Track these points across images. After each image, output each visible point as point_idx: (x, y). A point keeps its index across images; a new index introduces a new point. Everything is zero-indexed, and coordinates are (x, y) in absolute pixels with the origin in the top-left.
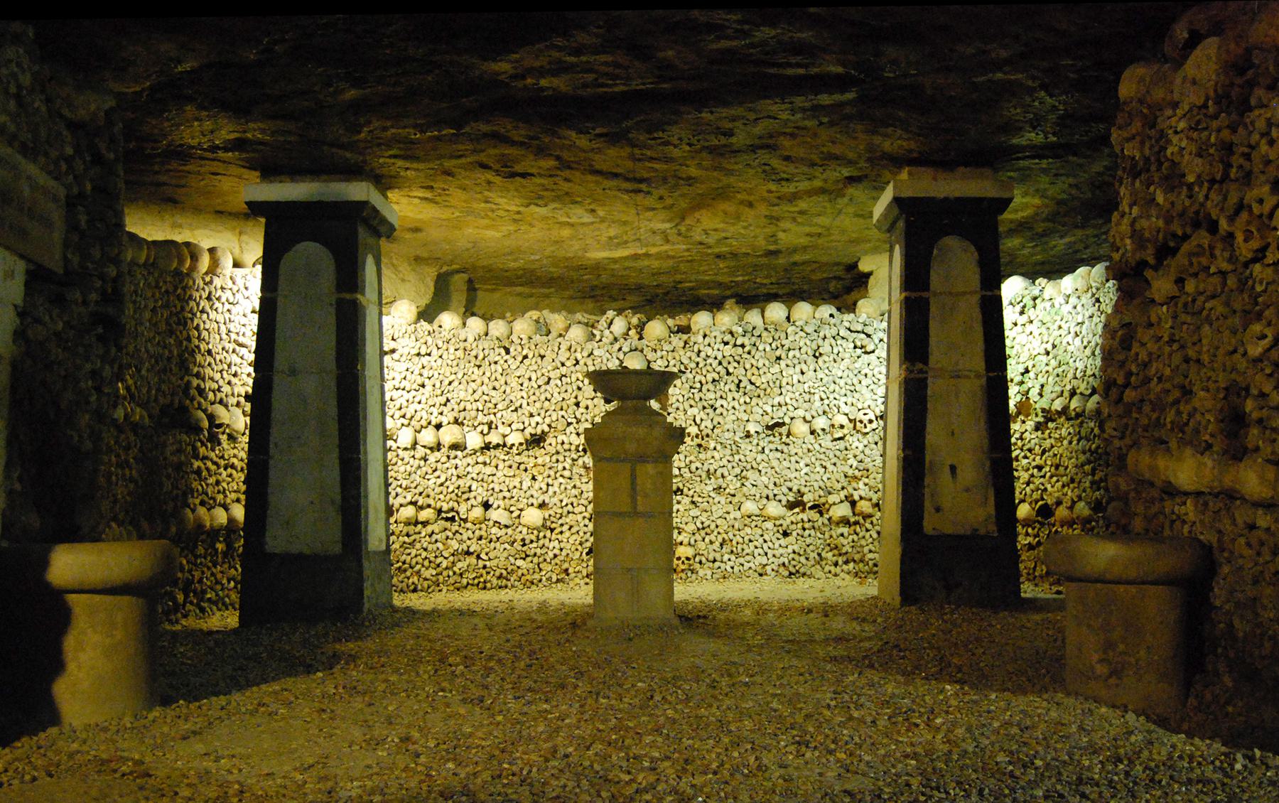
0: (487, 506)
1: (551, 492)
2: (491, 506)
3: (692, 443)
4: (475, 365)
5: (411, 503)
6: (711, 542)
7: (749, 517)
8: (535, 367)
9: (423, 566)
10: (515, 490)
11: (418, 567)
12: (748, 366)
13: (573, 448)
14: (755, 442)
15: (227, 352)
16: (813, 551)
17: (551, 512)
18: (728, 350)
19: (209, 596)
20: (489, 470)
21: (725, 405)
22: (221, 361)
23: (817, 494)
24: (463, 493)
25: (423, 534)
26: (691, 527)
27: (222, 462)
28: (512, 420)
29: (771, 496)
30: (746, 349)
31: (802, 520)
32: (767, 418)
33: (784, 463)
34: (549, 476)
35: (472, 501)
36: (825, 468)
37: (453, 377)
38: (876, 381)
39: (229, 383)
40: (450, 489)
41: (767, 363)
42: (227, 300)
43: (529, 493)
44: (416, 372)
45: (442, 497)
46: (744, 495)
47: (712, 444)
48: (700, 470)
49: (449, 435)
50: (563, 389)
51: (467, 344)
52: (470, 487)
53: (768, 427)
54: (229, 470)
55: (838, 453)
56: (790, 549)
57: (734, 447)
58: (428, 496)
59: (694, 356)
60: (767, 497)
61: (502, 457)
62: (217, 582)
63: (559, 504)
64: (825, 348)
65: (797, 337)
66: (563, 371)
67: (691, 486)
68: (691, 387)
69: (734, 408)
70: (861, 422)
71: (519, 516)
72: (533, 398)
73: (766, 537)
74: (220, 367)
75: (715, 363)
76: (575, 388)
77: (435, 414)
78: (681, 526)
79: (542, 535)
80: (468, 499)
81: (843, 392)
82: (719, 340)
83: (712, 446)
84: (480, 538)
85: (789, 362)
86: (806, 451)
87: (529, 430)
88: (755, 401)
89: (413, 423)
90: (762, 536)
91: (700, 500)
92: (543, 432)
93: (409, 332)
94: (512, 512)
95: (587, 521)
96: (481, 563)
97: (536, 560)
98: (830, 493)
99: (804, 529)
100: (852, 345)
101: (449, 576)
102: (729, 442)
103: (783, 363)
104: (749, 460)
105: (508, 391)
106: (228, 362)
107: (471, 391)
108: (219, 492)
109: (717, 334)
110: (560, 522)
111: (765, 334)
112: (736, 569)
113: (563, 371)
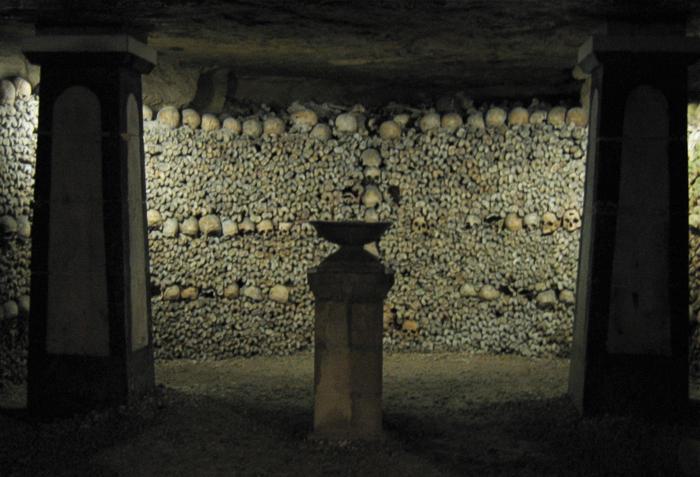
0: (240, 283)
1: (295, 272)
2: (244, 284)
4: (230, 162)
5: (176, 283)
6: (434, 318)
7: (467, 297)
8: (283, 163)
9: (186, 336)
10: (265, 271)
11: (182, 337)
12: (470, 165)
14: (474, 232)
15: (14, 170)
16: (521, 331)
17: (296, 289)
19: (5, 374)
20: (242, 253)
21: (449, 199)
22: (8, 179)
24: (220, 273)
25: (186, 310)
26: (416, 305)
27: (13, 263)
29: (487, 280)
31: (513, 304)
32: (485, 212)
34: (294, 258)
35: (229, 280)
36: (535, 259)
37: (211, 173)
39: (16, 196)
40: (209, 270)
41: (486, 163)
42: (12, 126)
43: (276, 273)
44: (179, 170)
45: (202, 277)
46: (463, 279)
47: (437, 234)
48: (425, 256)
49: (208, 223)
50: (308, 182)
52: (226, 268)
54: (19, 269)
55: (546, 247)
56: (501, 328)
57: (456, 236)
58: (190, 277)
60: (483, 281)
61: (254, 242)
62: (13, 361)
63: (302, 282)
64: (538, 153)
65: (514, 141)
66: (308, 166)
68: (420, 183)
69: (456, 202)
70: (568, 220)
71: (268, 292)
72: (280, 191)
73: (482, 316)
74: (8, 184)
75: (441, 162)
76: (317, 181)
77: (196, 206)
79: (288, 308)
80: (224, 278)
81: (552, 193)
82: (445, 141)
83: (437, 234)
84: (235, 311)
85: (506, 164)
86: (518, 242)
88: (475, 196)
89: (176, 215)
90: (478, 314)
91: (425, 281)
93: (172, 135)
94: (262, 289)
96: (235, 333)
97: (282, 329)
98: (537, 282)
99: (514, 311)
100: (561, 151)
101: (208, 344)
103: (500, 165)
104: (468, 248)
105: (259, 184)
106: (15, 177)
107: (226, 185)
108: (10, 288)
109: (443, 135)
110: (304, 297)
112: (455, 342)
113: (308, 166)
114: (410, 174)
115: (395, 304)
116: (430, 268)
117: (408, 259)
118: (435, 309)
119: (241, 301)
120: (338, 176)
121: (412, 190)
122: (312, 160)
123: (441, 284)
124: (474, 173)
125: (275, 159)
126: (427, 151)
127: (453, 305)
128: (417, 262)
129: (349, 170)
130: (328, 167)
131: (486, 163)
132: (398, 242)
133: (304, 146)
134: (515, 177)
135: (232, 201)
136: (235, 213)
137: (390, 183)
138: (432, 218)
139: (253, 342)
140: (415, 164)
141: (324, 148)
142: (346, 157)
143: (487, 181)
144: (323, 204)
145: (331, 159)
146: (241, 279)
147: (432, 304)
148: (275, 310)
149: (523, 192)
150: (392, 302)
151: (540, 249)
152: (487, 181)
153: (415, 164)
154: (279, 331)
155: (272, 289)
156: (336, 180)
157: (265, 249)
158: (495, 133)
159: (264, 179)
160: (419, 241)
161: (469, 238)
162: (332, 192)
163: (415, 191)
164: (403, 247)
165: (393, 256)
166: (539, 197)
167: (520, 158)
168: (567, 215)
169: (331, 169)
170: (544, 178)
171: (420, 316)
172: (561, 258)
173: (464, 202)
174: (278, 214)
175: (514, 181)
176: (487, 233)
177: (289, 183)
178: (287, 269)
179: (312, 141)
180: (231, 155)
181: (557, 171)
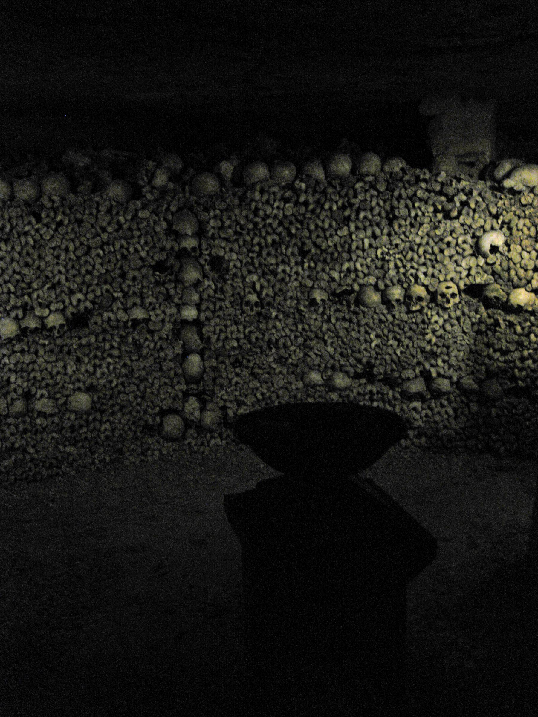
0: (28, 396)
1: (98, 374)
8: (72, 236)
10: (59, 377)
12: (312, 227)
13: (121, 324)
14: (321, 310)
20: (27, 359)
21: (288, 269)
23: (389, 368)
26: (250, 400)
29: (337, 365)
30: (311, 207)
32: (334, 285)
34: (96, 357)
36: (399, 341)
38: (460, 251)
41: (334, 223)
43: (74, 378)
46: (308, 365)
48: (260, 343)
52: (8, 379)
55: (414, 327)
60: (333, 368)
61: (42, 341)
66: (105, 236)
68: (250, 251)
69: (297, 273)
70: (443, 295)
79: (91, 417)
80: (8, 393)
81: (422, 260)
82: (279, 196)
83: (274, 314)
84: (25, 431)
85: (360, 224)
86: (377, 321)
87: (70, 309)
88: (320, 266)
91: (260, 372)
92: (86, 308)
94: (57, 399)
96: (28, 457)
97: (86, 445)
100: (431, 209)
102: (292, 310)
104: (314, 329)
110: (110, 403)
111: (330, 190)
113: (105, 236)
114: (237, 240)
115: (225, 401)
116: (267, 355)
117: (240, 347)
120: (146, 248)
121: (241, 261)
122: (110, 229)
123: (280, 373)
124: (318, 236)
125: (62, 230)
126: (257, 209)
128: (251, 349)
129: (159, 240)
131: (334, 223)
133: (98, 211)
135: (9, 292)
136: (14, 307)
137: (213, 253)
139: (51, 464)
140: (242, 228)
142: (155, 222)
143: (335, 245)
145: (135, 227)
146: (30, 390)
147: (270, 397)
149: (383, 259)
150: (222, 399)
151: (407, 329)
152: (335, 245)
153: (242, 228)
154: (83, 446)
156: (143, 254)
157: (56, 350)
158: (341, 185)
159: (49, 258)
160: (251, 324)
161: (314, 317)
162: (139, 269)
164: (232, 333)
165: (220, 344)
166: (404, 266)
167: (378, 218)
168: (442, 288)
169: (136, 240)
170: (410, 242)
172: (434, 340)
173: (307, 273)
174: (71, 303)
175: (371, 246)
176: (337, 310)
178: (87, 371)
179: (107, 204)
181: (428, 235)
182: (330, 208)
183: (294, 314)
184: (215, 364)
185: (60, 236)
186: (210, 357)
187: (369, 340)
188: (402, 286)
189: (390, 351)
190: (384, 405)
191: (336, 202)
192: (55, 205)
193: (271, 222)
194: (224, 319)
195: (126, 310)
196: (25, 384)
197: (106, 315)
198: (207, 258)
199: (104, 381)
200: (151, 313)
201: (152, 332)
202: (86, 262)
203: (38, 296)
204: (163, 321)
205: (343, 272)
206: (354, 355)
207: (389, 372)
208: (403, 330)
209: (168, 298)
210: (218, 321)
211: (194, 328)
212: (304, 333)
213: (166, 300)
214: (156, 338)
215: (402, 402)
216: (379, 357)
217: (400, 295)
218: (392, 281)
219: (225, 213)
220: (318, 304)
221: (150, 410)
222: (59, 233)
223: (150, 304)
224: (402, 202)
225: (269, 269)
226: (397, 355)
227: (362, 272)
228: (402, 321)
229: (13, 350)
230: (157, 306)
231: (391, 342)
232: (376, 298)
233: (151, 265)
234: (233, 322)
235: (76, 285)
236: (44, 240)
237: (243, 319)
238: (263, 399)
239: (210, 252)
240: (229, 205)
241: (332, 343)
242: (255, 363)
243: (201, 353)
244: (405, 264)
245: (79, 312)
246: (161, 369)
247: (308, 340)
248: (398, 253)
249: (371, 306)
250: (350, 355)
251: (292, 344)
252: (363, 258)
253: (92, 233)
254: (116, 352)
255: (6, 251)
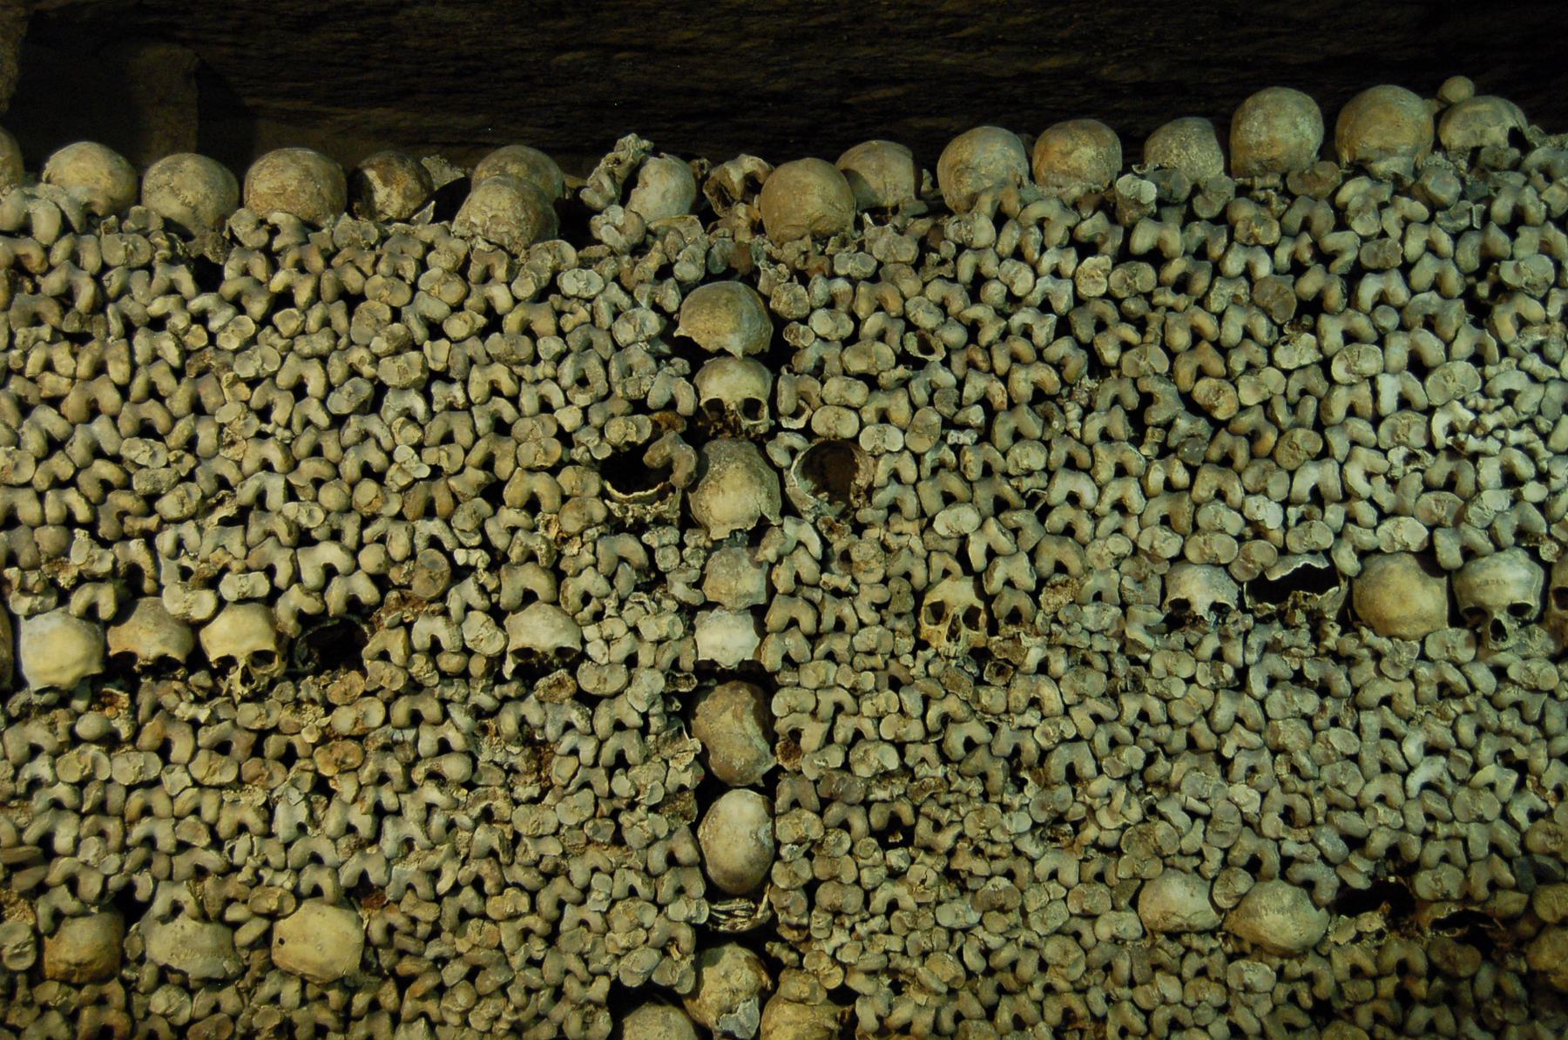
1: (389, 843)
3: (952, 649)
7: (1173, 936)
8: (322, 343)
10: (242, 844)
12: (1181, 339)
13: (477, 666)
14: (1210, 644)
18: (1096, 275)
20: (125, 768)
23: (1479, 877)
28: (219, 557)
29: (1271, 860)
32: (1261, 552)
33: (1335, 736)
34: (383, 779)
35: (62, 899)
36: (1522, 768)
41: (1262, 326)
43: (298, 850)
46: (1159, 853)
48: (979, 759)
50: (436, 429)
51: (30, 251)
52: (46, 840)
53: (1261, 588)
57: (1120, 664)
59: (957, 302)
60: (1254, 866)
61: (185, 710)
63: (423, 889)
65: (1391, 221)
66: (438, 354)
67: (945, 816)
68: (948, 424)
69: (1120, 507)
71: (265, 940)
75: (1043, 330)
76: (482, 424)
78: (905, 964)
79: (360, 1001)
80: (42, 888)
82: (1057, 234)
83: (1033, 657)
85: (1361, 323)
86: (1429, 691)
87: (294, 599)
88: (1208, 481)
91: (980, 867)
92: (353, 603)
94: (235, 926)
95: (537, 948)
102: (1100, 644)
103: (1332, 330)
104: (1181, 715)
107: (33, 441)
109: (1050, 209)
110: (433, 950)
111: (1244, 211)
113: (438, 354)
114: (904, 383)
117: (906, 770)
118: (1026, 985)
119: (129, 986)
120: (582, 399)
121: (917, 458)
122: (456, 327)
125: (287, 320)
127: (1108, 968)
130: (535, 360)
132: (855, 692)
133: (423, 266)
134: (1413, 385)
137: (818, 427)
138: (1009, 583)
141: (512, 273)
143: (1266, 404)
144: (513, 530)
145: (543, 322)
146: (130, 887)
148: (298, 1016)
149: (1454, 452)
152: (1266, 404)
155: (282, 926)
156: (569, 418)
157: (241, 743)
162: (554, 471)
163: (929, 460)
165: (835, 757)
166: (1543, 477)
169: (545, 369)
171: (958, 1017)
173: (1160, 507)
174: (296, 578)
175: (1404, 403)
176: (1267, 648)
177: (350, 433)
178: (350, 829)
179: (461, 247)
180: (66, 299)
182: (1248, 273)
183: (1105, 654)
184: (815, 832)
185: (275, 339)
186: (795, 804)
187: (1401, 761)
188: (1534, 554)
189: (1488, 806)
190: (1458, 1023)
191: (1271, 250)
192: (277, 244)
193: (1029, 321)
194: (851, 664)
195: (497, 614)
196: (113, 861)
197: (427, 628)
198: (798, 442)
199: (413, 867)
200: (590, 632)
201: (587, 700)
202: (365, 436)
203: (179, 544)
204: (631, 661)
205: (1297, 504)
206: (1339, 818)
207: (1482, 892)
208: (1540, 724)
209: (652, 579)
210: (830, 671)
211: (744, 694)
212: (1145, 730)
213: (648, 588)
214: (603, 723)
215: (1533, 1016)
216: (1442, 830)
217: (1529, 583)
218: (1494, 538)
219: (863, 289)
220: (1197, 620)
221: (572, 987)
222: (276, 329)
223: (586, 598)
224: (1528, 237)
225: (1017, 489)
226: (1514, 825)
227: (1371, 501)
228: (1536, 690)
229: (71, 731)
230: (611, 604)
231: (1490, 772)
232: (1428, 598)
233: (594, 460)
234: (884, 682)
235: (319, 515)
236: (217, 349)
237: (917, 670)
238: (989, 972)
239: (809, 422)
240: (880, 264)
241: (1253, 770)
242: (961, 836)
243: (767, 787)
244: (1544, 465)
245: (325, 611)
246: (618, 840)
247: (1161, 758)
248: (1518, 427)
249: (1404, 631)
250: (1320, 819)
251: (1100, 771)
252: (1377, 447)
253: (392, 337)
254: (454, 767)
255: (73, 378)
